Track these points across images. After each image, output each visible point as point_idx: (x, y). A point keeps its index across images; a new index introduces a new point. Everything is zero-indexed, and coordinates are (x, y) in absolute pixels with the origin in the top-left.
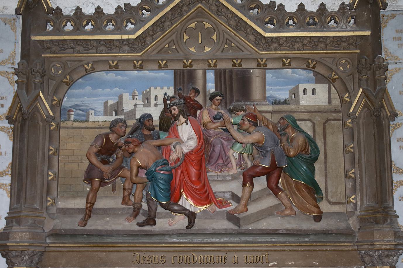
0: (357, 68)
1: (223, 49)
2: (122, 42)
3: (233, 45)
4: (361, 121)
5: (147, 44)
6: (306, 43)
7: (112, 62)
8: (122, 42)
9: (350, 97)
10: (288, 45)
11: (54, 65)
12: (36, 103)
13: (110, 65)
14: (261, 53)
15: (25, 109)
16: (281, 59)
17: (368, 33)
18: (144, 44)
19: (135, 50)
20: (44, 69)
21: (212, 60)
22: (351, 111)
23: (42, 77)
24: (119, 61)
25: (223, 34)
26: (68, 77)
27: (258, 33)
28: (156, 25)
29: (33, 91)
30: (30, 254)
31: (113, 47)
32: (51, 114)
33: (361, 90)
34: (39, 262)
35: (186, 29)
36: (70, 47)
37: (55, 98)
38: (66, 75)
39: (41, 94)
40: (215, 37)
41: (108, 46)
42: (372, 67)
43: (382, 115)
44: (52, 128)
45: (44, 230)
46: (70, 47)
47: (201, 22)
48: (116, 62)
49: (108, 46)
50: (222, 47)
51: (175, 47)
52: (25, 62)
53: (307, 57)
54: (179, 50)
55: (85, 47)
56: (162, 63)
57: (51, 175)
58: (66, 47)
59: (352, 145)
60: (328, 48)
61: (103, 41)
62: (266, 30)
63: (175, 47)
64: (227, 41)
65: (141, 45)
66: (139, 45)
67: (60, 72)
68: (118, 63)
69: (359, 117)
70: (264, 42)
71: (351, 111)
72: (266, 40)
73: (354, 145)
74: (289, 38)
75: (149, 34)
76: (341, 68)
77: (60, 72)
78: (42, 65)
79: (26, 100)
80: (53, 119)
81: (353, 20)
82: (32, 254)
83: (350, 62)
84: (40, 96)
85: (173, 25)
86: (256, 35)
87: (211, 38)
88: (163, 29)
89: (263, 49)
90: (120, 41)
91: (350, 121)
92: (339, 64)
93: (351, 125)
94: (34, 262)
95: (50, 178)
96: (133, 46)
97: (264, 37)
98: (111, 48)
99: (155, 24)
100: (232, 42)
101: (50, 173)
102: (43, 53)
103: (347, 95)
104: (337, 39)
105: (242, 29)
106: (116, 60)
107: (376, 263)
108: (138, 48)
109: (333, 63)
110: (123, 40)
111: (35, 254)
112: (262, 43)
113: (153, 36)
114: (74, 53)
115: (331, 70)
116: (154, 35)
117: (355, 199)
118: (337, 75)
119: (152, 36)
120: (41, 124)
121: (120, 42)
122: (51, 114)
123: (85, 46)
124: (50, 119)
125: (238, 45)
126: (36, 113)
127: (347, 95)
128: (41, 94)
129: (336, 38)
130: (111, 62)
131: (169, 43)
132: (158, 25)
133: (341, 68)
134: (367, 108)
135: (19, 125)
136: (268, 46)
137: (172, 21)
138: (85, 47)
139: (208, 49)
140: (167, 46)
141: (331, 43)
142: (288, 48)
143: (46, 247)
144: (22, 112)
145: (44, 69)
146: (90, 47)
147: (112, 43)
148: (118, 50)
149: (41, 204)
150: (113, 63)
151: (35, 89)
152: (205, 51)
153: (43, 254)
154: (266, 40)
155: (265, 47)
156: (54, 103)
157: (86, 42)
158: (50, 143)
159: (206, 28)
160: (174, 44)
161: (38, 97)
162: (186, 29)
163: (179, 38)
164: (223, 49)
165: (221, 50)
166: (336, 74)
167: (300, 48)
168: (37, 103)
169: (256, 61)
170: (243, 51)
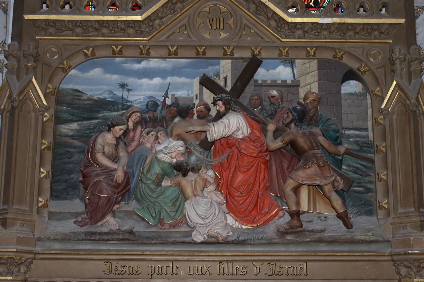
0: (389, 59)
1: (241, 35)
2: (127, 24)
3: (252, 31)
4: (395, 117)
5: (156, 28)
6: (333, 31)
7: (116, 47)
8: (128, 24)
9: (382, 91)
10: (313, 32)
11: (50, 49)
12: (27, 91)
13: (114, 51)
14: (283, 40)
15: (15, 95)
16: (305, 48)
17: (402, 21)
18: (152, 28)
19: (141, 34)
20: (37, 52)
21: (229, 47)
22: (383, 106)
23: (35, 61)
24: (123, 46)
25: (241, 18)
26: (65, 62)
27: (281, 18)
28: (166, 7)
29: (25, 77)
30: (18, 262)
31: (117, 30)
32: (45, 103)
33: (395, 83)
34: (28, 271)
35: (199, 13)
36: (69, 28)
37: (50, 86)
38: (63, 60)
39: (34, 80)
40: (231, 22)
41: (111, 28)
42: (407, 58)
43: (417, 111)
44: (45, 119)
45: (34, 235)
46: (69, 28)
47: (215, 5)
48: (120, 47)
49: (111, 28)
50: (240, 34)
51: (187, 33)
52: (16, 43)
53: (334, 46)
54: (191, 35)
55: (86, 29)
56: (172, 49)
57: (43, 173)
58: (64, 29)
59: (384, 145)
60: (357, 36)
61: (106, 23)
62: (291, 15)
63: (187, 33)
64: (246, 27)
65: (149, 29)
66: (146, 28)
67: (56, 57)
68: (122, 48)
69: (393, 113)
70: (286, 29)
71: (383, 106)
72: (289, 26)
73: (386, 144)
74: (315, 25)
75: (158, 17)
76: (372, 60)
77: (56, 57)
78: (36, 47)
79: (17, 86)
80: (47, 109)
81: (384, 10)
82: (20, 262)
83: (382, 53)
84: (33, 82)
85: (185, 8)
86: (278, 21)
87: (226, 23)
88: (174, 12)
89: (286, 37)
90: (125, 22)
91: (382, 117)
92: (369, 55)
93: (382, 122)
94: (22, 270)
95: (42, 176)
96: (139, 30)
97: (288, 23)
98: (115, 31)
99: (165, 6)
100: (250, 28)
101: (42, 170)
102: (38, 35)
103: (378, 89)
104: (368, 27)
105: (263, 13)
106: (120, 45)
107: (413, 275)
108: (145, 32)
109: (362, 53)
110: (128, 22)
111: (23, 261)
112: (285, 30)
113: (163, 20)
114: (72, 35)
115: (360, 60)
116: (164, 17)
117: (388, 203)
118: (368, 66)
119: (161, 18)
120: (33, 115)
121: (125, 24)
122: (45, 103)
123: (85, 28)
124: (43, 109)
125: (258, 31)
126: (28, 101)
127: (378, 89)
128: (34, 80)
129: (367, 26)
130: (114, 47)
131: (180, 28)
132: (168, 7)
133: (372, 60)
134: (401, 103)
135: (8, 114)
136: (291, 33)
137: (185, 4)
138: (86, 29)
139: (223, 35)
140: (178, 31)
141: (361, 32)
142: (313, 36)
143: (36, 254)
144: (11, 99)
145: (37, 52)
146: (91, 30)
147: (116, 26)
148: (123, 33)
149: (31, 205)
150: (117, 48)
151: (27, 74)
152: (220, 38)
153: (32, 262)
154: (289, 26)
155: (288, 34)
156: (48, 91)
157: (87, 24)
158: (43, 137)
159: (221, 12)
160: (186, 29)
161: (31, 84)
162: (199, 13)
163: (191, 23)
164: (241, 35)
165: (238, 37)
166: (366, 65)
167: (327, 36)
168: (29, 91)
169: (278, 50)
170: (262, 38)
